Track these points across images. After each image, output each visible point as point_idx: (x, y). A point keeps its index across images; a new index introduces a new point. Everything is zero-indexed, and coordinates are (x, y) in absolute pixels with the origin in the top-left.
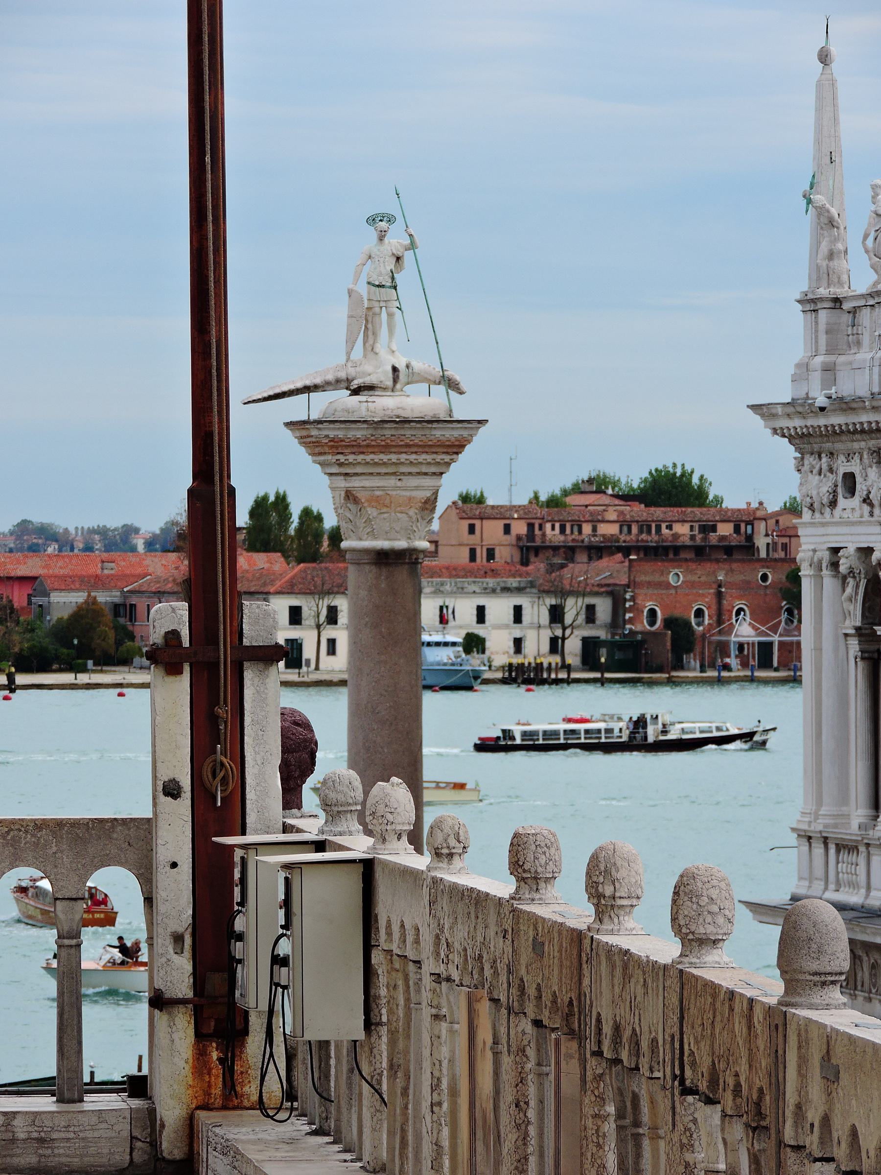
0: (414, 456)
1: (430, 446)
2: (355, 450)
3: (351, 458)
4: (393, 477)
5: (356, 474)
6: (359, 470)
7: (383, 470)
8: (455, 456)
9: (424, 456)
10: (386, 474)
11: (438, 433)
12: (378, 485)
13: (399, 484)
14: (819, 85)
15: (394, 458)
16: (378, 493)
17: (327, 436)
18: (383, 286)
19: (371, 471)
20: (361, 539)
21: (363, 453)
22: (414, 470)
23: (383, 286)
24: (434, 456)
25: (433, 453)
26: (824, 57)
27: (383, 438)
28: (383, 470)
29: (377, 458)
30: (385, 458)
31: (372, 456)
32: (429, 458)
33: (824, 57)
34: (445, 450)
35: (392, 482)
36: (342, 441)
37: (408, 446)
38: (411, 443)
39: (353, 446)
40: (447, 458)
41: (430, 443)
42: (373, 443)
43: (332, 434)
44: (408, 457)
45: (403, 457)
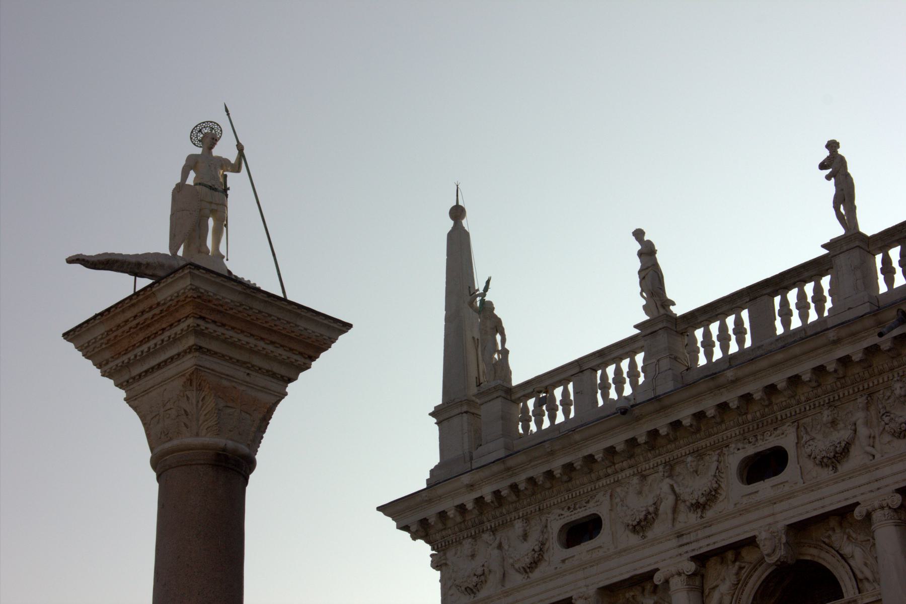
0: (270, 348)
1: (291, 338)
2: (218, 318)
3: (212, 327)
4: (242, 369)
5: (209, 352)
6: (214, 346)
7: (236, 354)
8: (307, 361)
9: (280, 351)
10: (238, 361)
11: (302, 324)
12: (228, 373)
13: (248, 379)
14: (450, 235)
15: (252, 341)
16: (225, 383)
17: (196, 289)
18: (215, 190)
19: (224, 352)
20: (197, 435)
21: (223, 325)
22: (265, 365)
23: (215, 190)
24: (289, 354)
25: (291, 350)
26: (457, 213)
27: (250, 312)
28: (236, 354)
29: (236, 336)
30: (244, 339)
31: (231, 333)
32: (285, 354)
33: (457, 213)
34: (302, 350)
35: (240, 373)
36: (209, 301)
37: (270, 331)
38: (275, 328)
39: (220, 312)
40: (301, 360)
41: (292, 335)
42: (240, 315)
43: (204, 287)
44: (266, 346)
45: (261, 344)
